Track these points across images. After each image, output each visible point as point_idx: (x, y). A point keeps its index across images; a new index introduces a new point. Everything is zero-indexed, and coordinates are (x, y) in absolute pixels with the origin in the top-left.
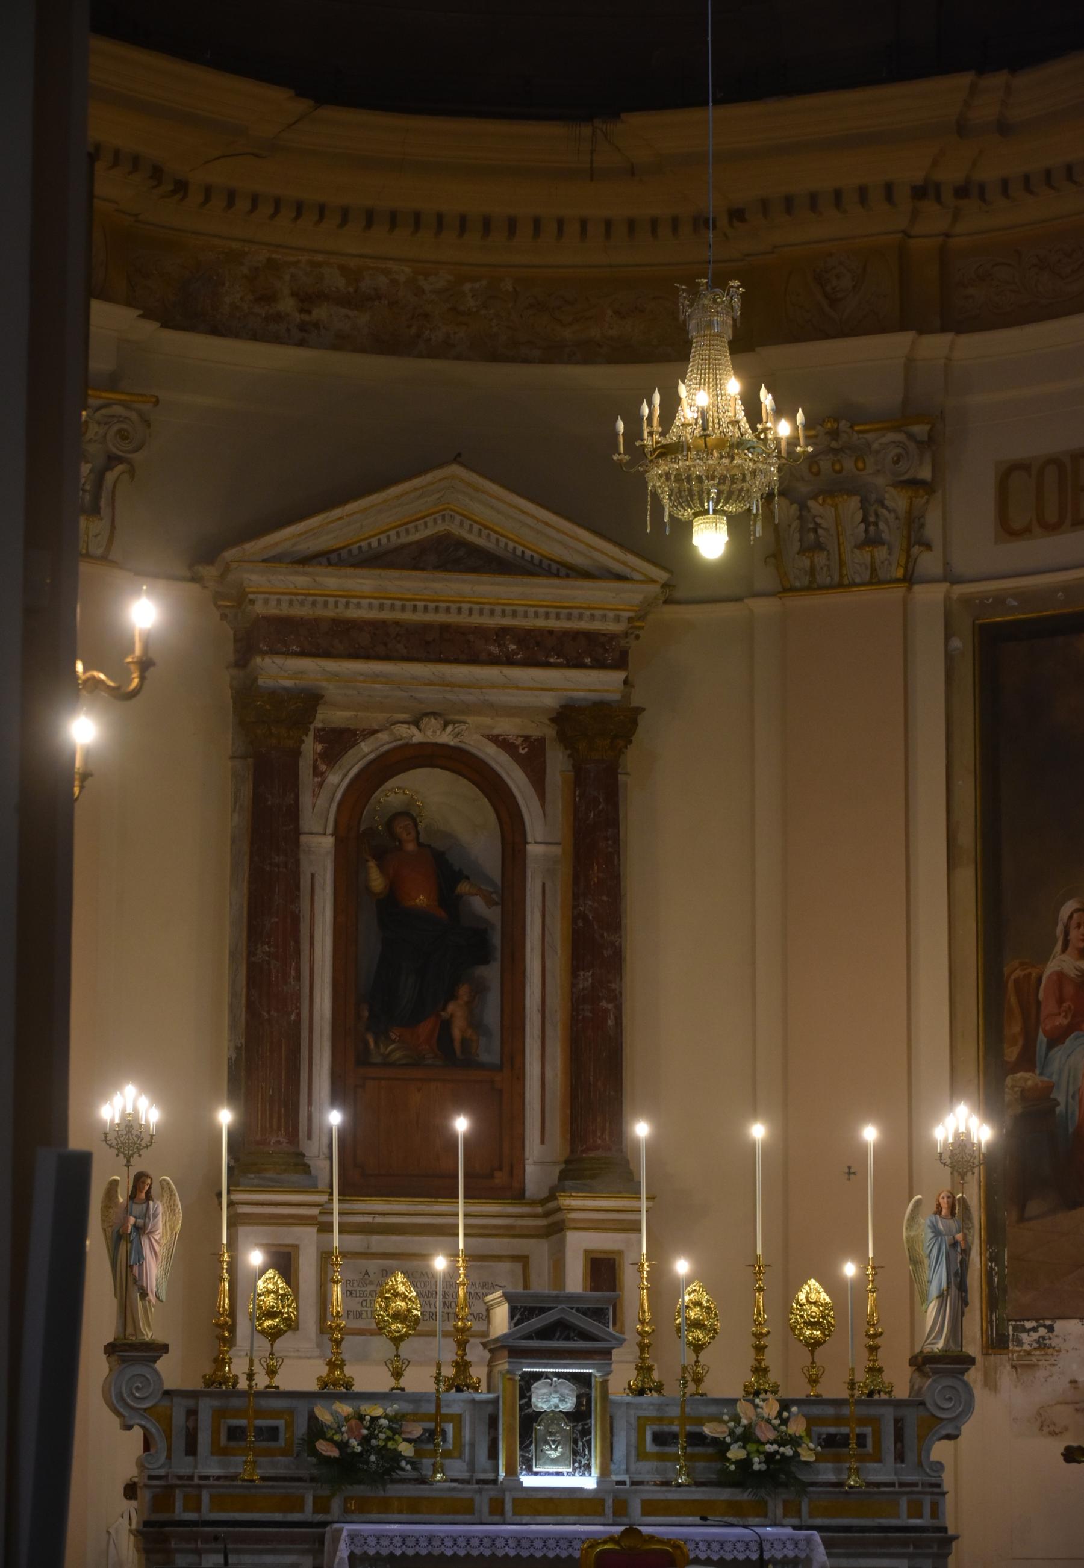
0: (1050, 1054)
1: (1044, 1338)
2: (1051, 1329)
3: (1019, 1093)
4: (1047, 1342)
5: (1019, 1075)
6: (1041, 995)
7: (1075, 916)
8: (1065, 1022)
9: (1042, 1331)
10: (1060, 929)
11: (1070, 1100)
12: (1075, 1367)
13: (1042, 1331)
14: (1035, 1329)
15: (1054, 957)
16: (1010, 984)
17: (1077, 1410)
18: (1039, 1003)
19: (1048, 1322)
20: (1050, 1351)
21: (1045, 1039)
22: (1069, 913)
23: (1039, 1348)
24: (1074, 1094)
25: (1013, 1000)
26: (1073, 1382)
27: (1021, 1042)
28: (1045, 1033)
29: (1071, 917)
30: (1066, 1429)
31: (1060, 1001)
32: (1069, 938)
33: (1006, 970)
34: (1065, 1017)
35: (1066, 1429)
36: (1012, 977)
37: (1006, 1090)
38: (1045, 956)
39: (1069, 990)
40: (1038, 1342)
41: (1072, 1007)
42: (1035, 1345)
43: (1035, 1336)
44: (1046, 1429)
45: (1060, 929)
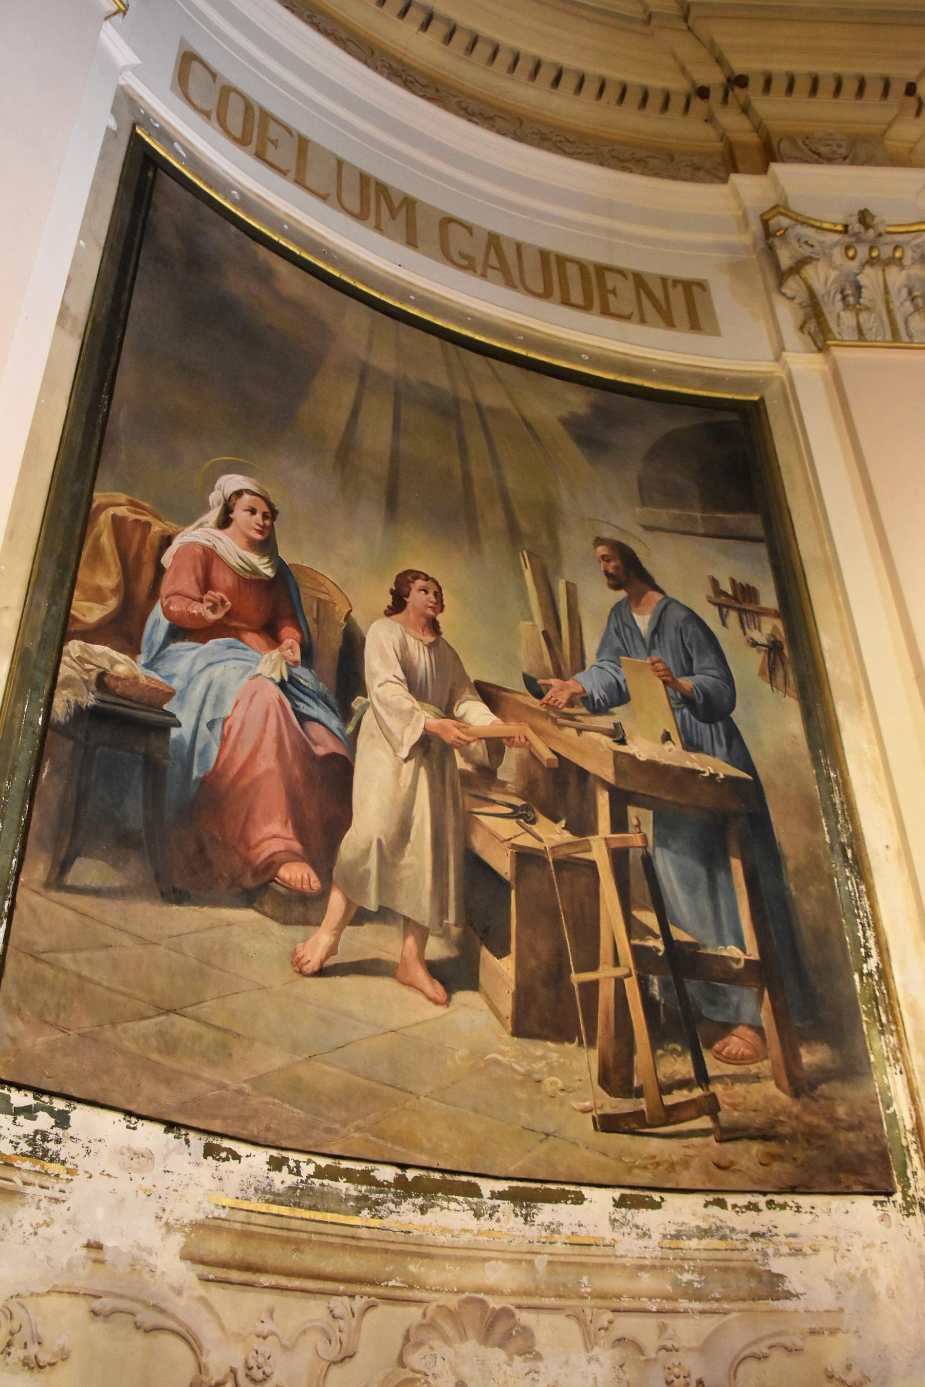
0: (172, 647)
1: (45, 1137)
2: (62, 1120)
3: (94, 675)
4: (51, 1146)
5: (99, 648)
6: (167, 559)
7: (246, 497)
8: (211, 617)
9: (44, 1121)
10: (215, 498)
11: (203, 727)
12: (100, 1213)
13: (44, 1121)
14: (29, 1112)
15: (200, 526)
16: (104, 518)
17: (95, 1313)
18: (160, 570)
19: (59, 1104)
20: (54, 1168)
21: (165, 623)
22: (236, 488)
23: (32, 1155)
24: (211, 725)
25: (107, 541)
26: (94, 1246)
27: (113, 603)
28: (167, 612)
29: (239, 494)
30: (64, 1356)
31: (206, 584)
32: (231, 516)
33: (99, 497)
34: (214, 609)
35: (64, 1356)
36: (111, 511)
37: (65, 658)
38: (189, 518)
39: (224, 579)
40: (32, 1142)
41: (228, 603)
42: (25, 1148)
43: (28, 1126)
44: (17, 1352)
45: (215, 498)
